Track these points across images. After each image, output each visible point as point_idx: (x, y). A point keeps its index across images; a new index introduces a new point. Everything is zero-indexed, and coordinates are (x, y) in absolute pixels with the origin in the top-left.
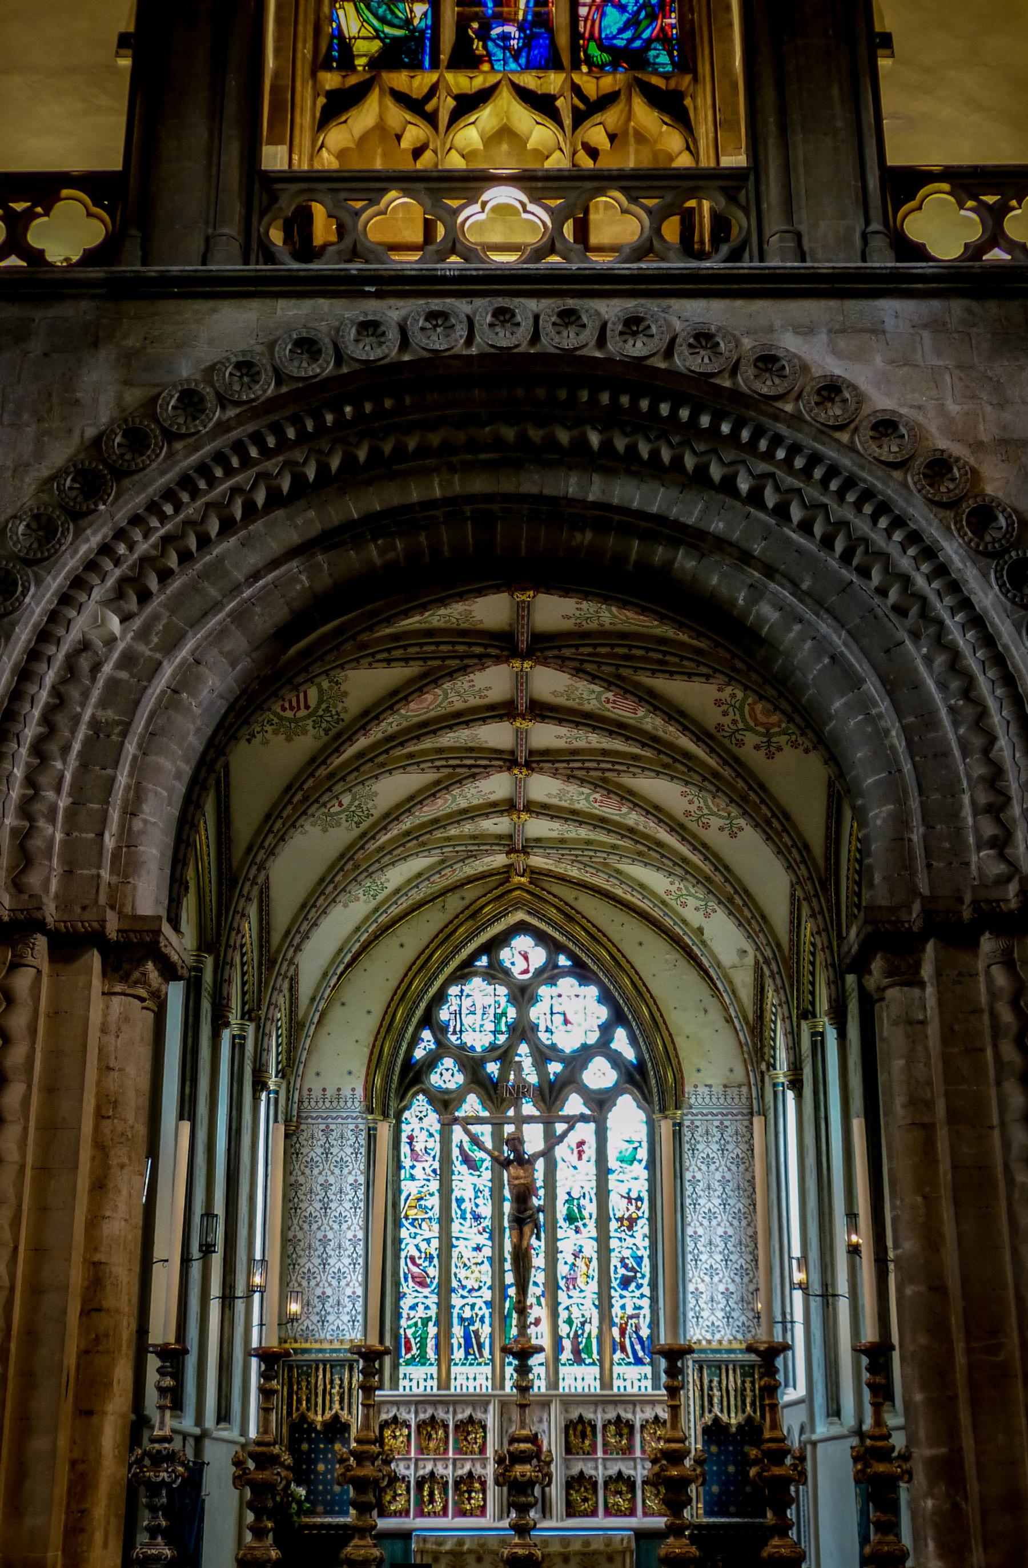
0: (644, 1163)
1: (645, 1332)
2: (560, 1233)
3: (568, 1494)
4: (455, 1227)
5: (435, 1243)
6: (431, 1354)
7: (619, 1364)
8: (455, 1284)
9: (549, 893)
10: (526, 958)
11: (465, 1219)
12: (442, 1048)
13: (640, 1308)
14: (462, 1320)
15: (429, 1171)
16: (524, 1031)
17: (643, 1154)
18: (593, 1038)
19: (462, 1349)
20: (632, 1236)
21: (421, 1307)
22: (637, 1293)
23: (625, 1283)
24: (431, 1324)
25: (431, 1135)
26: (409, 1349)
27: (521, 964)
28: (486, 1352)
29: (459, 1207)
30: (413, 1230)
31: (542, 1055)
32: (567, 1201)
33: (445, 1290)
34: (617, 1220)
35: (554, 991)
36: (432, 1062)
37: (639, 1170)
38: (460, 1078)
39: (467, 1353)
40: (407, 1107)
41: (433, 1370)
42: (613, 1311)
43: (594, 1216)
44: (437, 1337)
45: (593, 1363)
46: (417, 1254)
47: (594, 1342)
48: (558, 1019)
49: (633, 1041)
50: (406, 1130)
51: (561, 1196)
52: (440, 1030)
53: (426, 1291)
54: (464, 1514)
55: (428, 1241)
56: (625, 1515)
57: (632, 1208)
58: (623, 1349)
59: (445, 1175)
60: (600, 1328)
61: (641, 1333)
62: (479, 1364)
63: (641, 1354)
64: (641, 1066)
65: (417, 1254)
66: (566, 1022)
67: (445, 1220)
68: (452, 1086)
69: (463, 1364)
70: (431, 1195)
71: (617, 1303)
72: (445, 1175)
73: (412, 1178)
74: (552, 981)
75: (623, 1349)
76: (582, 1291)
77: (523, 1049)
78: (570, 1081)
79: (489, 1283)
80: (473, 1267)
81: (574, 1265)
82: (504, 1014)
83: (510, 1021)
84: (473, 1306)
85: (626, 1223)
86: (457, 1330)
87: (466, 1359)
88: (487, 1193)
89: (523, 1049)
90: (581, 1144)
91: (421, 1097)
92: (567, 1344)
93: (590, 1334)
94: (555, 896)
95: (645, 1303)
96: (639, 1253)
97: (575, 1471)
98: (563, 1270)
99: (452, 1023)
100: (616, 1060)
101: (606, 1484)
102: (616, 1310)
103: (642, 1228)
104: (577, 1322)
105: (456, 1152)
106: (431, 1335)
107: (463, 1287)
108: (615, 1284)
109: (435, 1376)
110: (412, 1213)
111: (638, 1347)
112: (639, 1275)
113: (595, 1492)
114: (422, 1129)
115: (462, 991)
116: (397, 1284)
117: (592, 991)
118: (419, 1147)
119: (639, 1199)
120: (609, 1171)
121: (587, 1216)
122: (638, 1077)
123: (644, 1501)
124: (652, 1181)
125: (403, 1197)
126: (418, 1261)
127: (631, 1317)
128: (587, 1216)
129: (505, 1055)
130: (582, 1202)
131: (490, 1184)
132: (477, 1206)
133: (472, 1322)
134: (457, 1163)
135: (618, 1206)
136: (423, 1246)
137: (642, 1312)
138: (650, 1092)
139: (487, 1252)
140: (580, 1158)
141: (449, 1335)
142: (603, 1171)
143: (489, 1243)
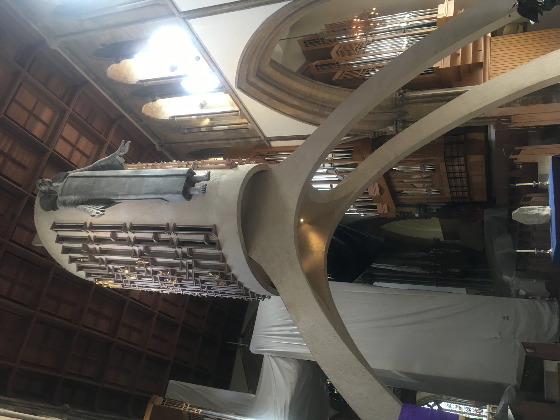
17: (449, 404)
23: (470, 410)
37: (452, 405)
49: (431, 402)
57: (458, 407)
58: (480, 413)
60: (477, 416)
64: (435, 401)
71: (473, 413)
100: (434, 405)
103: (461, 406)
108: (470, 412)
119: (457, 406)
120: (452, 410)
124: (454, 403)
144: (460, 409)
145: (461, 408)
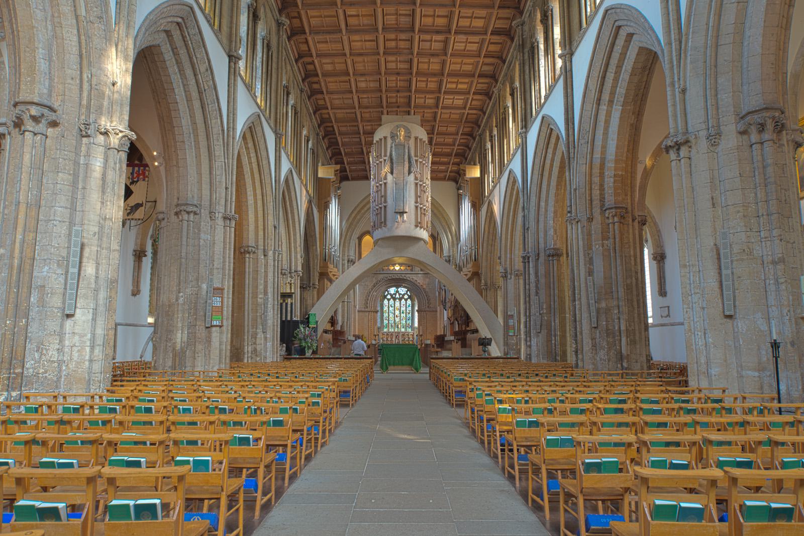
12: (388, 294)
31: (400, 294)
33: (389, 320)
36: (387, 295)
52: (388, 292)
59: (389, 308)
67: (389, 313)
72: (389, 308)
78: (403, 297)
100: (408, 295)
129: (395, 294)
135: (408, 311)
142: (406, 308)
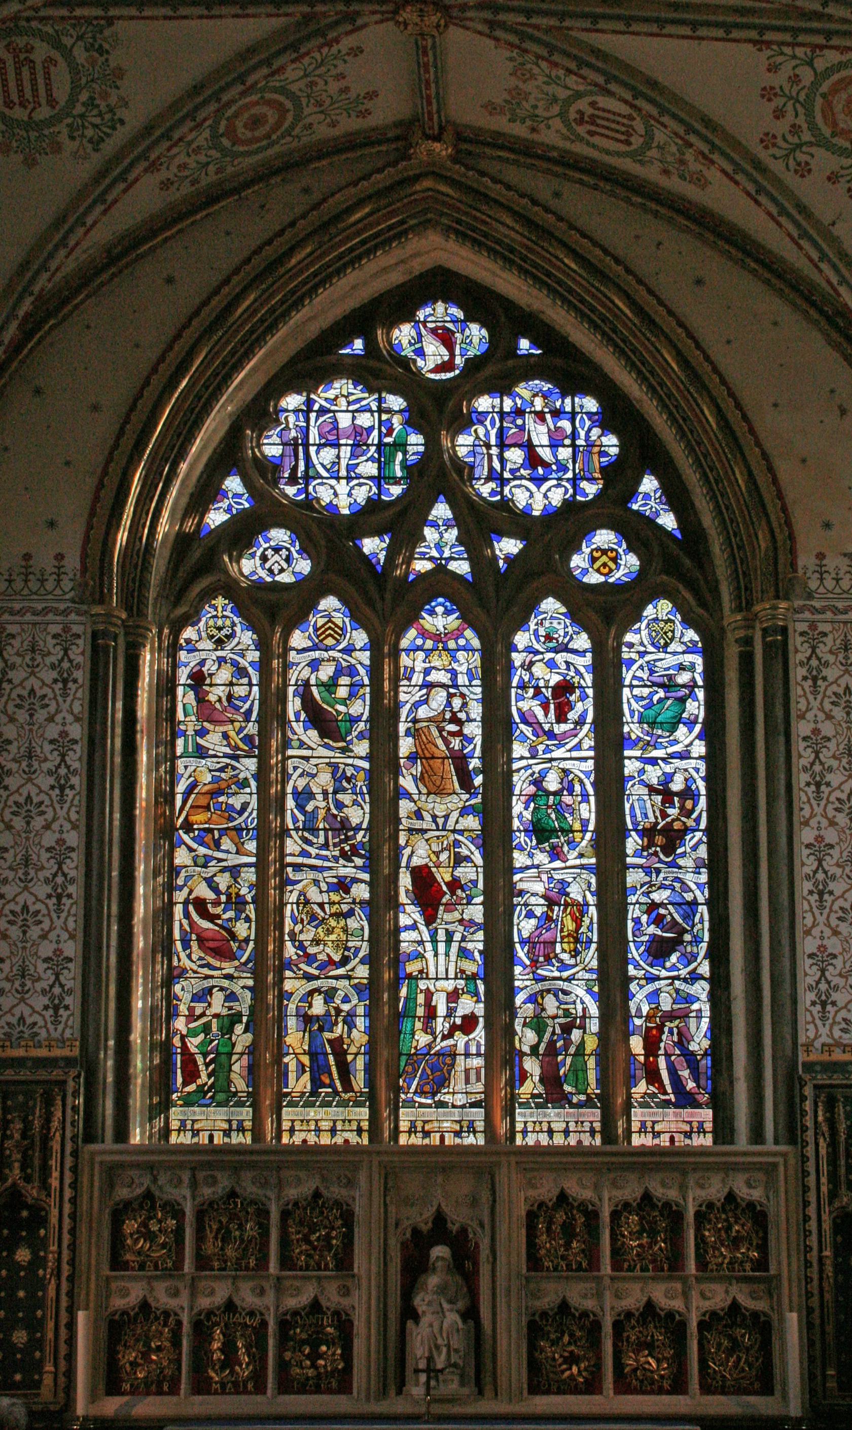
0: (698, 728)
1: (700, 1042)
2: (520, 859)
3: (532, 1347)
4: (292, 846)
5: (250, 875)
6: (240, 1084)
7: (644, 1105)
8: (290, 951)
9: (495, 181)
10: (449, 345)
11: (314, 831)
13: (690, 999)
14: (307, 1019)
15: (235, 739)
16: (442, 472)
17: (696, 708)
18: (591, 489)
19: (307, 1077)
20: (673, 865)
21: (218, 998)
22: (683, 973)
24: (239, 1029)
25: (241, 672)
26: (191, 1075)
27: (435, 352)
28: (359, 1081)
29: (301, 807)
30: (202, 850)
32: (532, 798)
34: (643, 833)
35: (508, 404)
38: (304, 566)
39: (316, 1083)
40: (191, 619)
41: (246, 1114)
42: (632, 1005)
43: (591, 827)
44: (252, 1050)
45: (588, 1103)
46: (210, 895)
47: (591, 1063)
48: (515, 456)
50: (187, 660)
51: (521, 784)
53: (229, 968)
54: (303, 1389)
55: (235, 871)
56: (661, 1391)
57: (673, 812)
58: (653, 1076)
60: (603, 1036)
61: (693, 1047)
62: (343, 1104)
63: (691, 1085)
65: (210, 895)
66: (533, 460)
68: (286, 578)
69: (309, 1105)
70: (244, 784)
73: (201, 752)
74: (503, 388)
75: (653, 1076)
76: (564, 967)
77: (441, 510)
79: (365, 950)
80: (333, 923)
81: (549, 919)
82: (401, 445)
83: (412, 459)
84: (329, 995)
85: (659, 839)
86: (295, 1038)
87: (314, 1093)
88: (361, 783)
89: (441, 510)
90: (564, 689)
91: (220, 601)
92: (532, 1066)
93: (582, 1045)
94: (509, 187)
95: (701, 989)
96: (689, 897)
97: (548, 1300)
98: (526, 927)
99: (288, 463)
101: (618, 1326)
102: (639, 1001)
104: (553, 1027)
105: (294, 705)
106: (239, 1049)
107: (310, 959)
108: (634, 953)
109: (248, 1125)
110: (199, 818)
111: (685, 1073)
112: (687, 937)
113: (595, 1343)
114: (221, 661)
115: (309, 403)
116: (164, 946)
117: (591, 404)
118: (216, 694)
119: (688, 793)
121: (577, 826)
122: (687, 562)
123: (703, 1362)
125: (181, 787)
126: (212, 910)
127: (671, 1016)
128: (577, 826)
130: (567, 799)
131: (366, 765)
132: (340, 805)
133: (325, 1022)
134: (298, 727)
136: (223, 881)
137: (695, 1006)
138: (715, 590)
139: (361, 892)
140: (561, 718)
141: (280, 1051)
143: (366, 877)
144: (648, 833)
145: (669, 849)
